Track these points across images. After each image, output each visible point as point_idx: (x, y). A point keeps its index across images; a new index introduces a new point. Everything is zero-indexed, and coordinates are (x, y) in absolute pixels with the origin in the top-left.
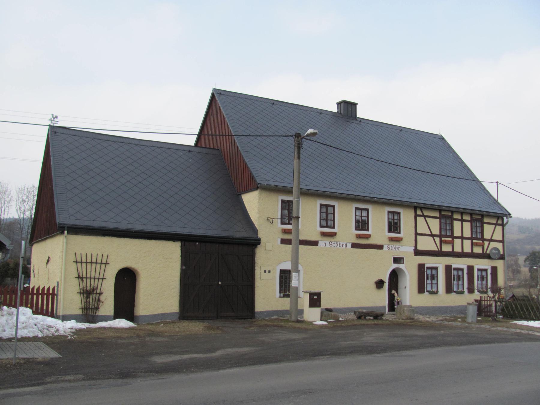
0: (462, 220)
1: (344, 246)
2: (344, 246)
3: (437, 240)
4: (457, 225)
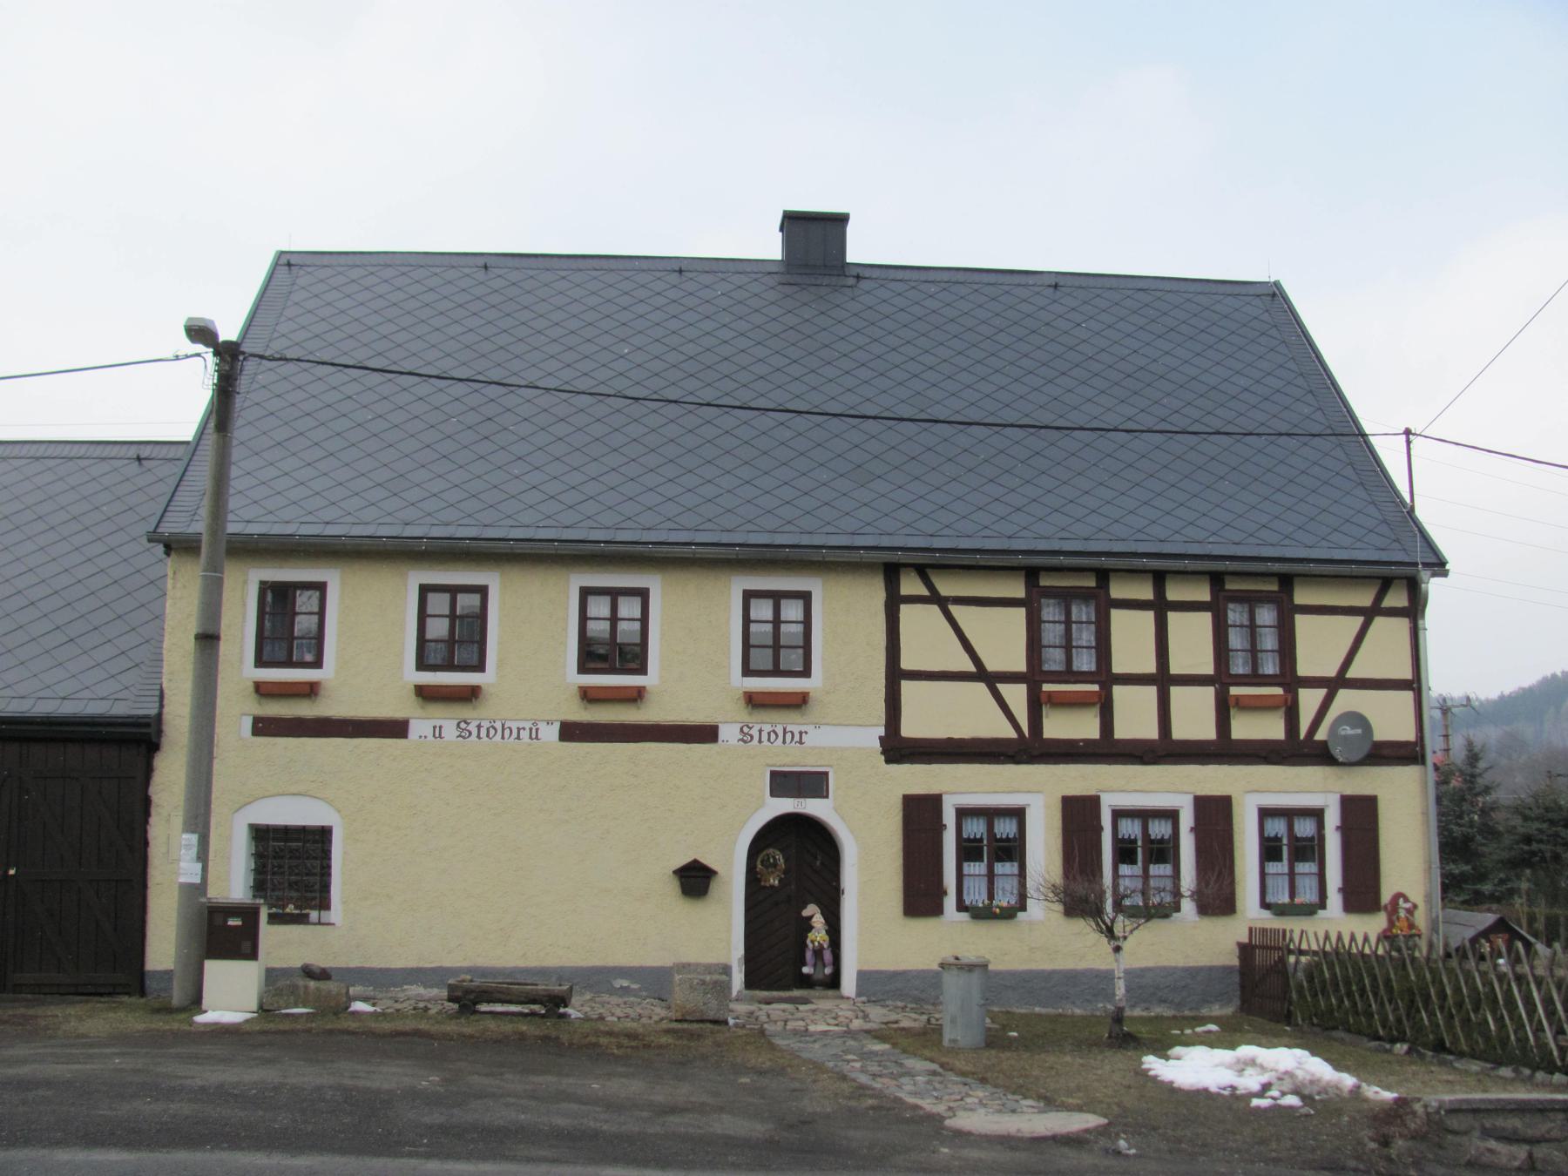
0: (1161, 608)
1: (525, 734)
2: (525, 734)
3: (1016, 696)
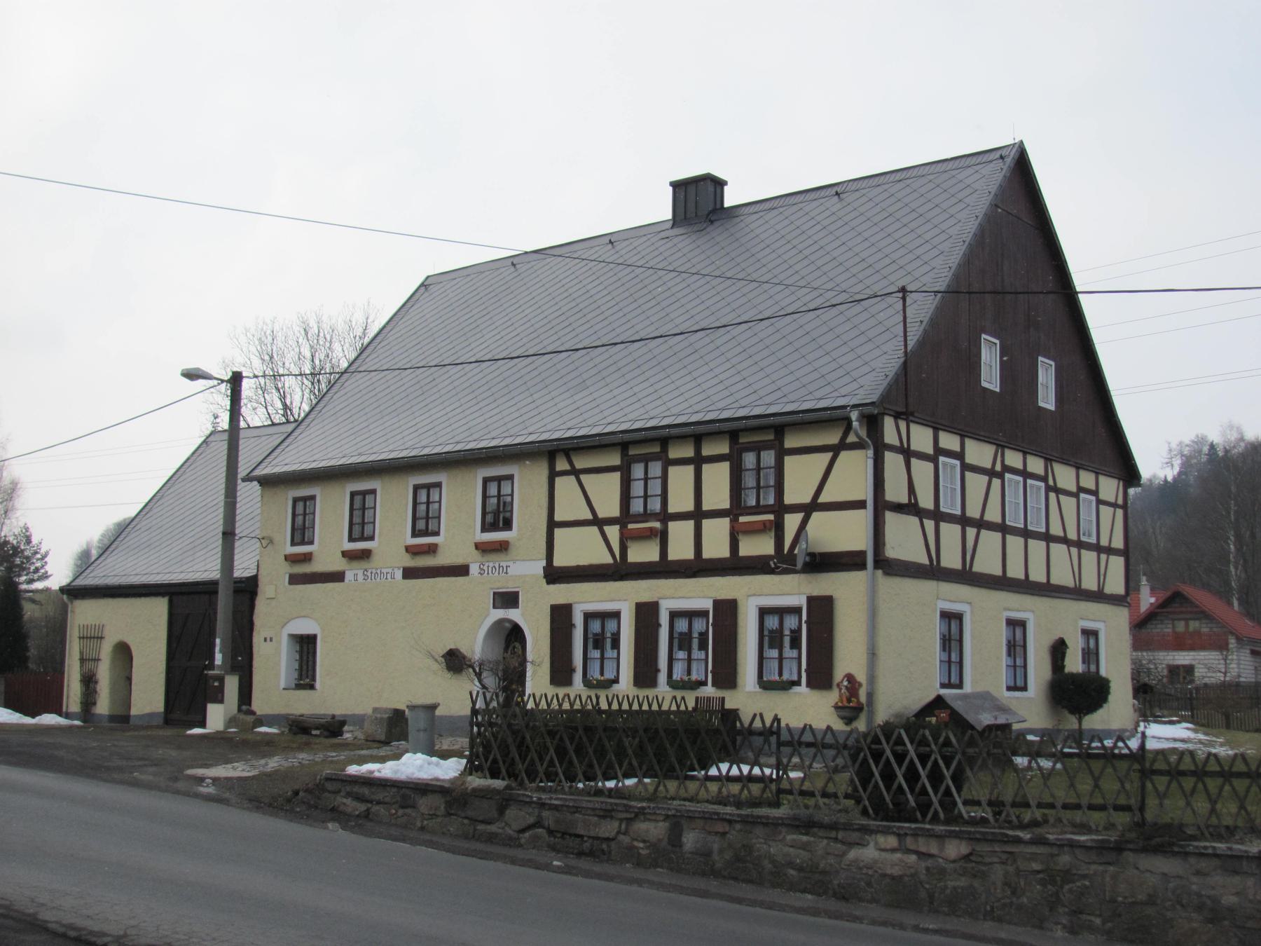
0: (698, 462)
1: (389, 576)
2: (389, 576)
3: (613, 532)
4: (681, 478)
